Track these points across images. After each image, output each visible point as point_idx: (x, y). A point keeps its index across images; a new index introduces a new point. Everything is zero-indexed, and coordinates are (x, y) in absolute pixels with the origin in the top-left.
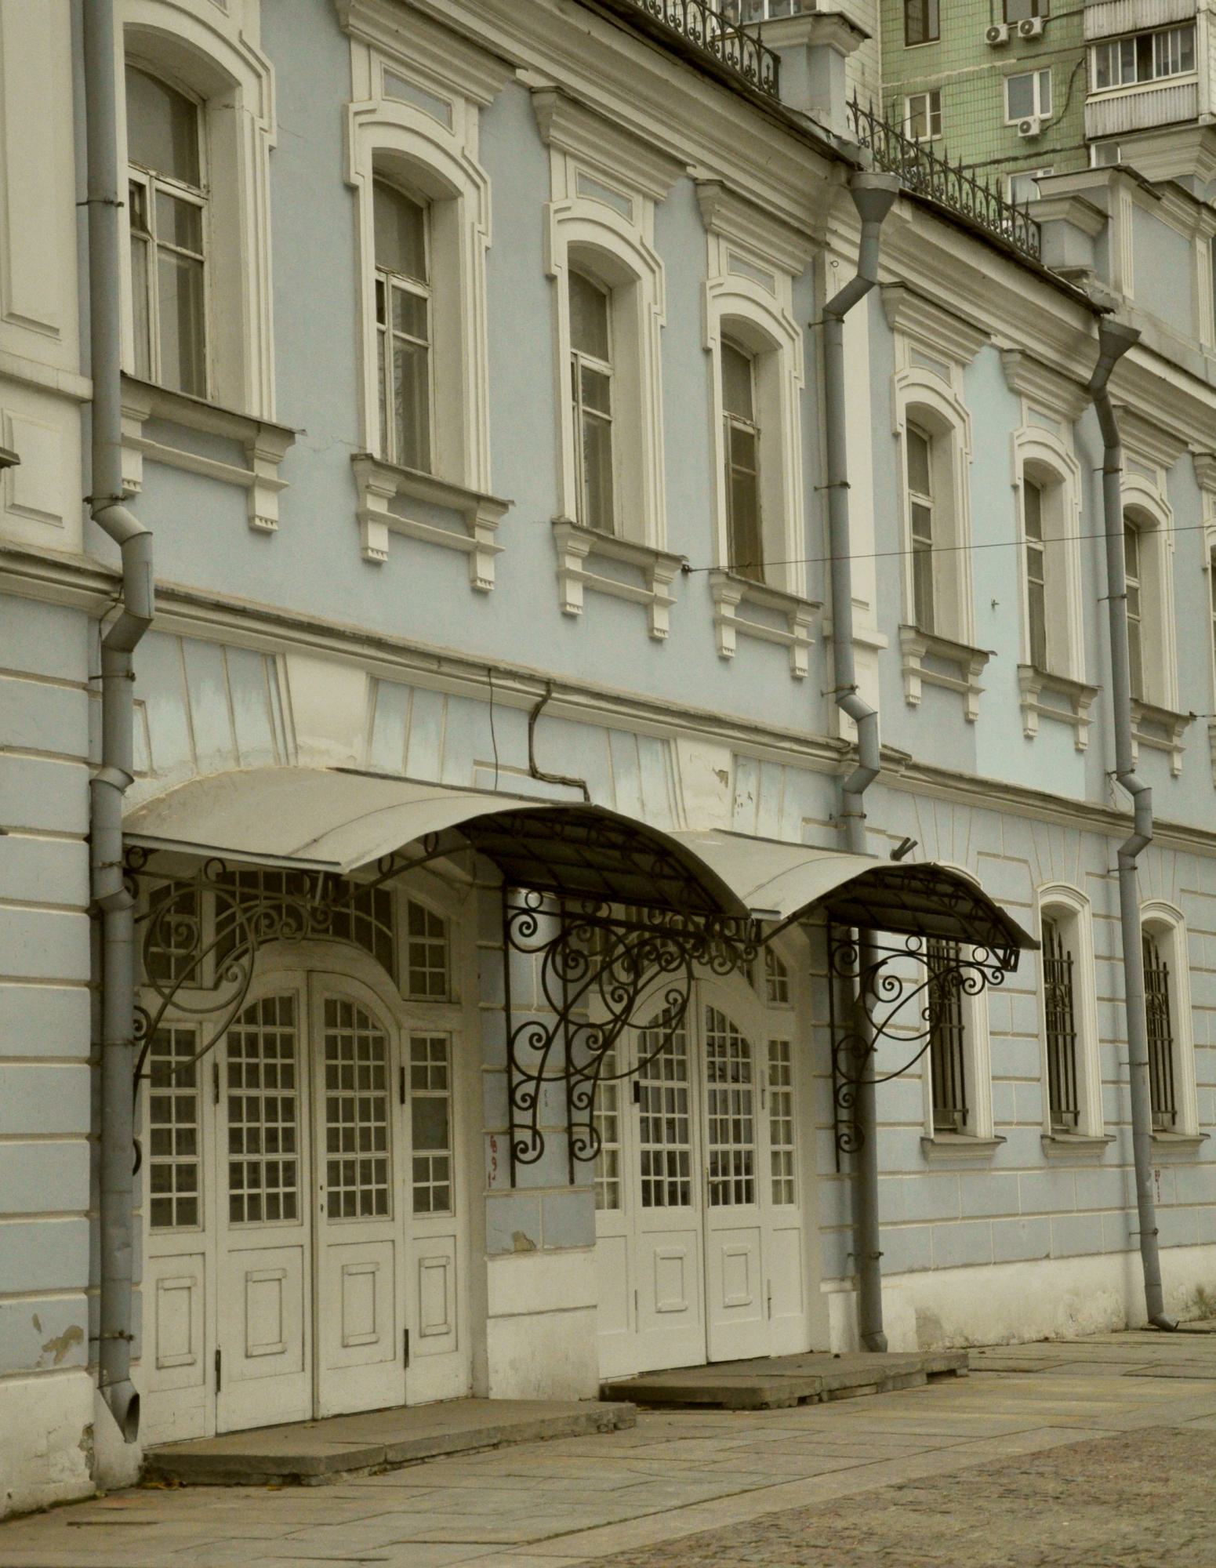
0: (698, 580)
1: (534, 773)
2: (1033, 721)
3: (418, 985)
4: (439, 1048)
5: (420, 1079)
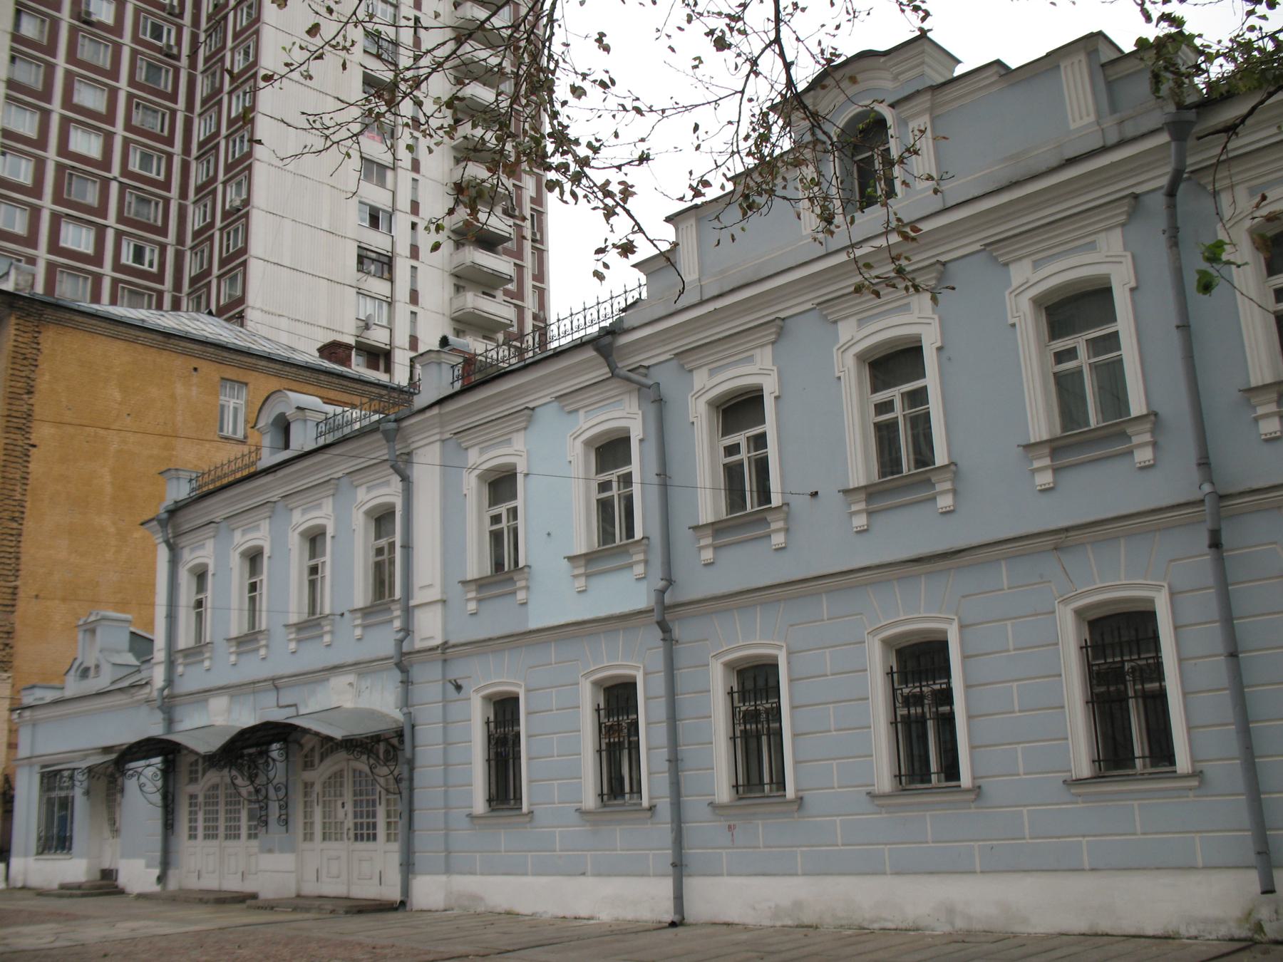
0: (347, 615)
1: (279, 707)
2: (581, 582)
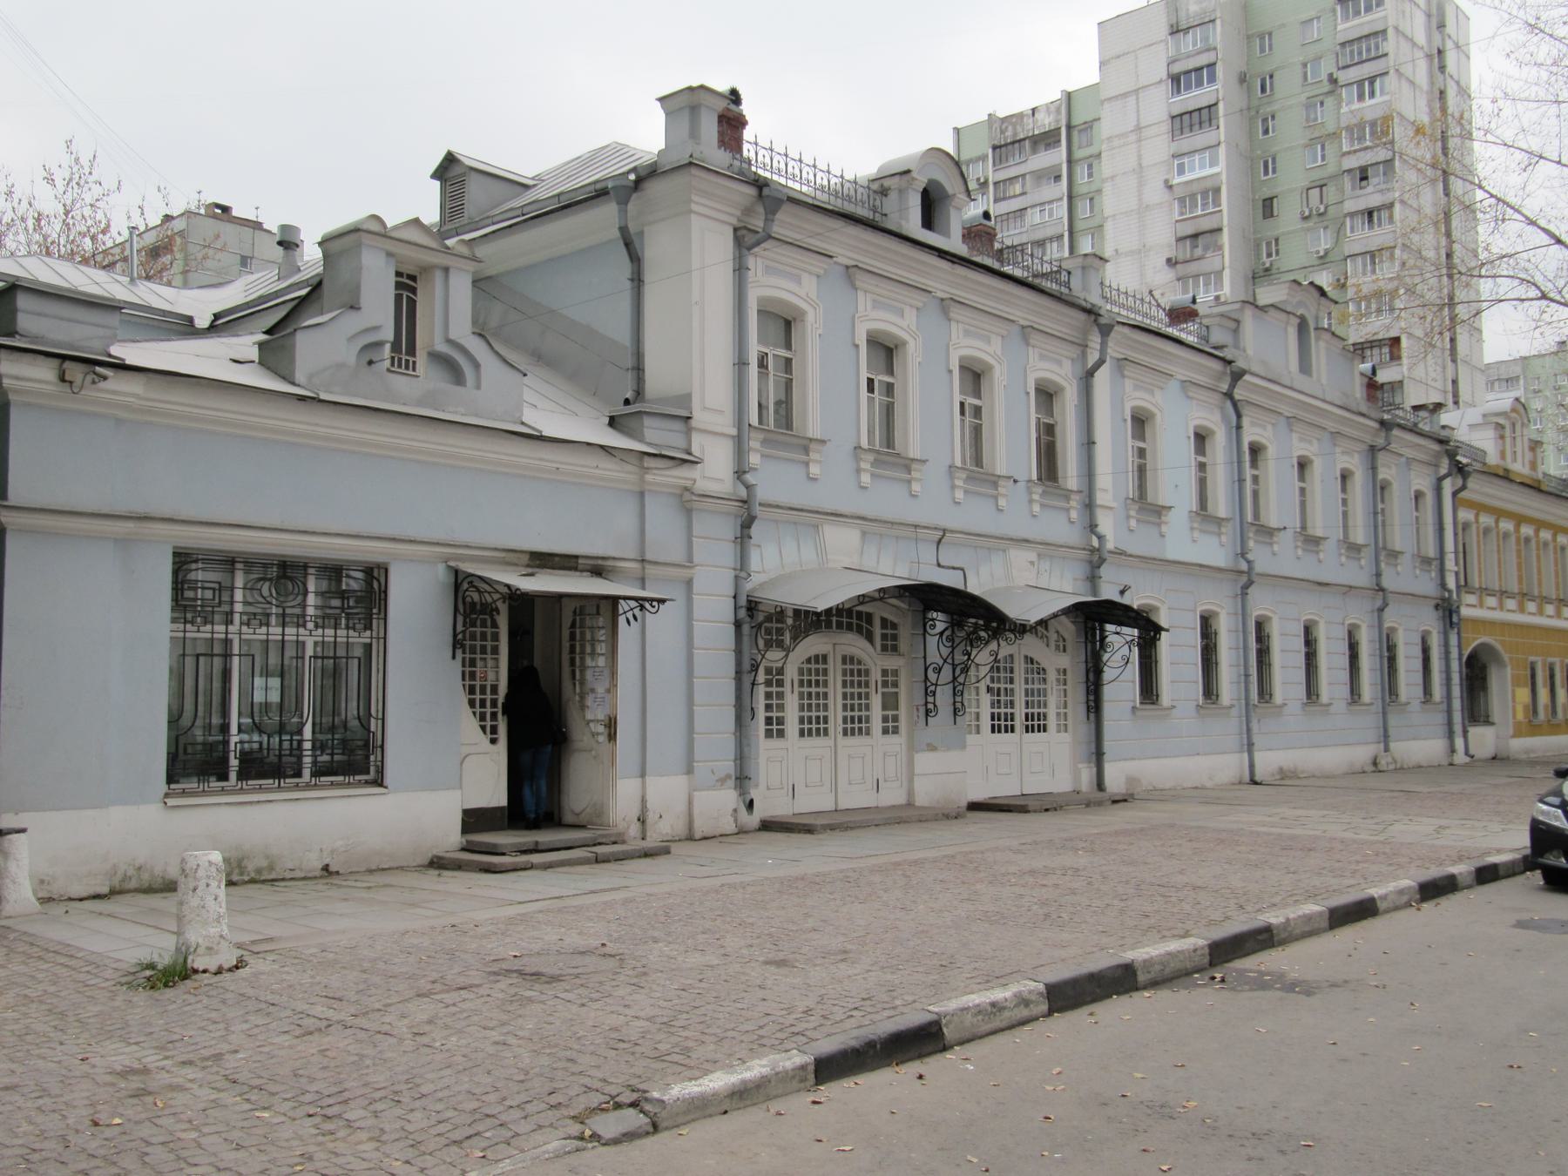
3: (884, 648)
4: (896, 673)
5: (885, 684)
